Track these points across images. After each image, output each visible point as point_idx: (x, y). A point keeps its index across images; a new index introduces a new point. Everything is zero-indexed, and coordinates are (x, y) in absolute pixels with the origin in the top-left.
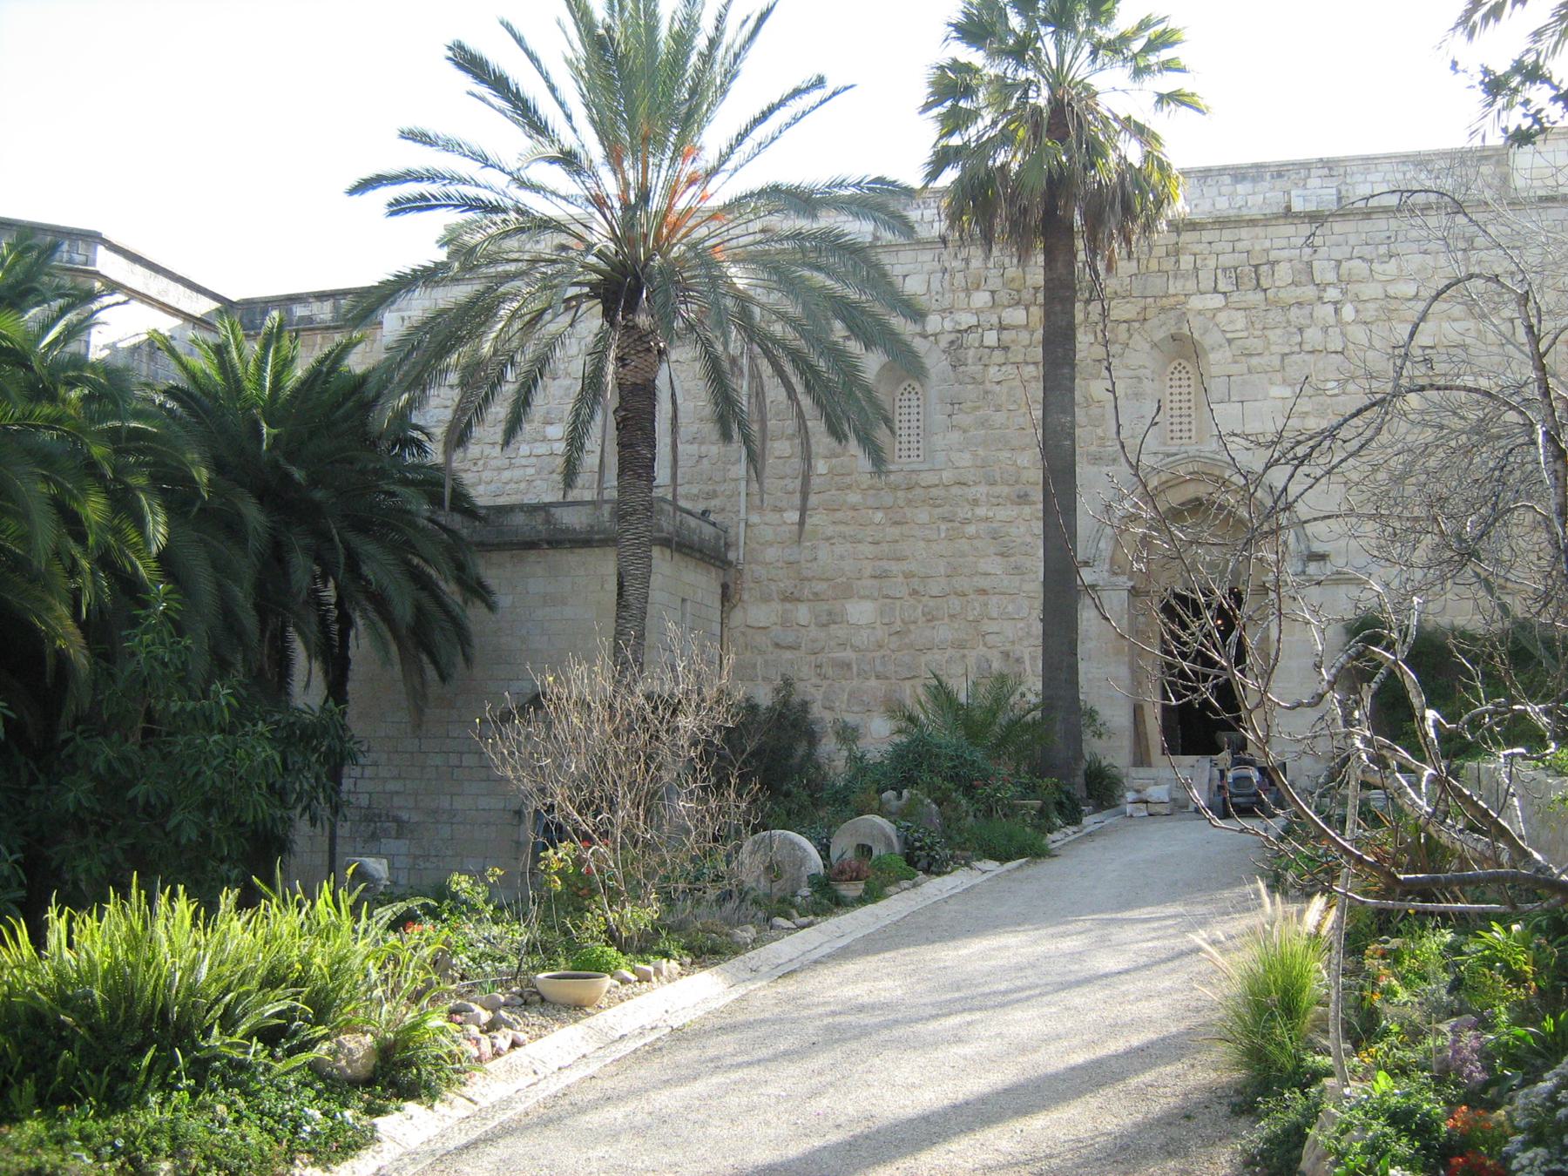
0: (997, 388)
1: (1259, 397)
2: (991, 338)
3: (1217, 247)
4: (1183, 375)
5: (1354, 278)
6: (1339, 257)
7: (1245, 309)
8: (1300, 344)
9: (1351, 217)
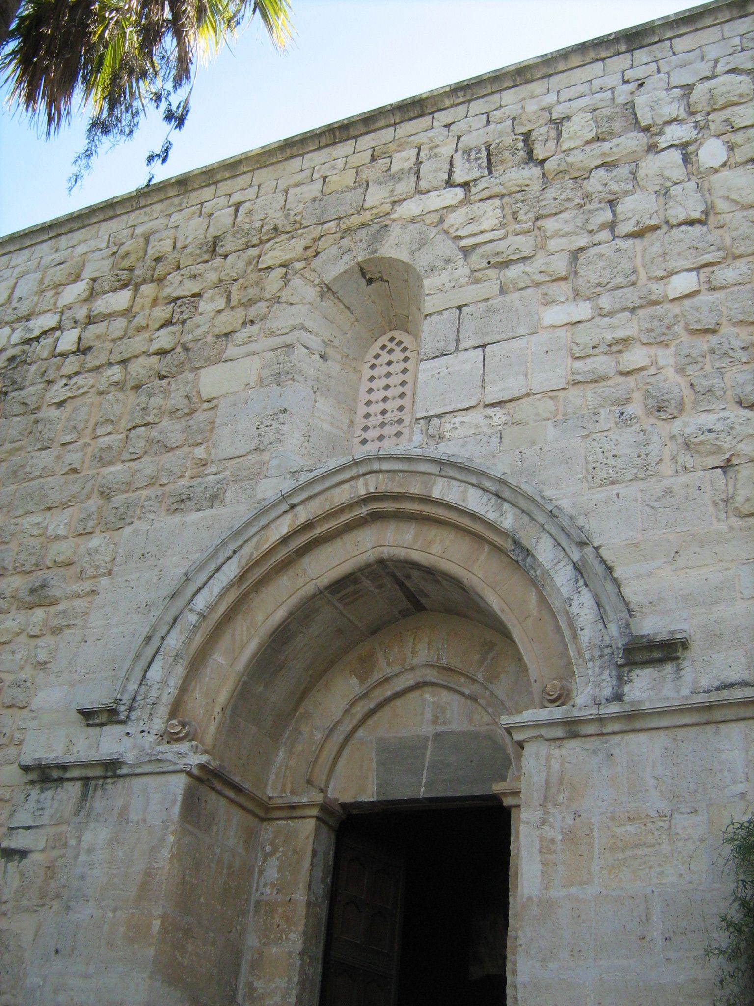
0: (54, 413)
1: (522, 331)
2: (68, 340)
3: (461, 126)
4: (398, 355)
5: (721, 101)
6: (689, 81)
7: (501, 196)
8: (612, 226)
9: (709, 21)
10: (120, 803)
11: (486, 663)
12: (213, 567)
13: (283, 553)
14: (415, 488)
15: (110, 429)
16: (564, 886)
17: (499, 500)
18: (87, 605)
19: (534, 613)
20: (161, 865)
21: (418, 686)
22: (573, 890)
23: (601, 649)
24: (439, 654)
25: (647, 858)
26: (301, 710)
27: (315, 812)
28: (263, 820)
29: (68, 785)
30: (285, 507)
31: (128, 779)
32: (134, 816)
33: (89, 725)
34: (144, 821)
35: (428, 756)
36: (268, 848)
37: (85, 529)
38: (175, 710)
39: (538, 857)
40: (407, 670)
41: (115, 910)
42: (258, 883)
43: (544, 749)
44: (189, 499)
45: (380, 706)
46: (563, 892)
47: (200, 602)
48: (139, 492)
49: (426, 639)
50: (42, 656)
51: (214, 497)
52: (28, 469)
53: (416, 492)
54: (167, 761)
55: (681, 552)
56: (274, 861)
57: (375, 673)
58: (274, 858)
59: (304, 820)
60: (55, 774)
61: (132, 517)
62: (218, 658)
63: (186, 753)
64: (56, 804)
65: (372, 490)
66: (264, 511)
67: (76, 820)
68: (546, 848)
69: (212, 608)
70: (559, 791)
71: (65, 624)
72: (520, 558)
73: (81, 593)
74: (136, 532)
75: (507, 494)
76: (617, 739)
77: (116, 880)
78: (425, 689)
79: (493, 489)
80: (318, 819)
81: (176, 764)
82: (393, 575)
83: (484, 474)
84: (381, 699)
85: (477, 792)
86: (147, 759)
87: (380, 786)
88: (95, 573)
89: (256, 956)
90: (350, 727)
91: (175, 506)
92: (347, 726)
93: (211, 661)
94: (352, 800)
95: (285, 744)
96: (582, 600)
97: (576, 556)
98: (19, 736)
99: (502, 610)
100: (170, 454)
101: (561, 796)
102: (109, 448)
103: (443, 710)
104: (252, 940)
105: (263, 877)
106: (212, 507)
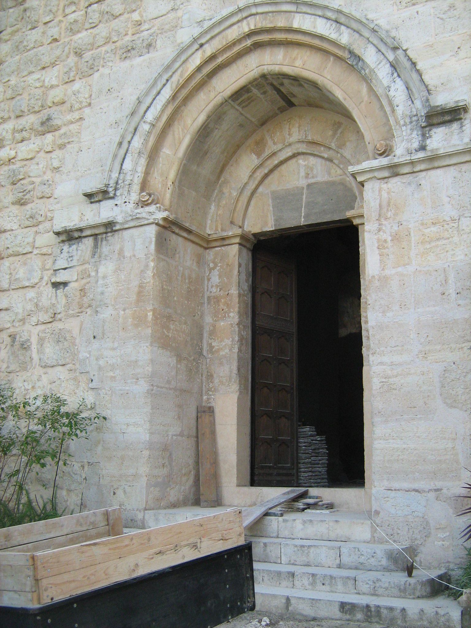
10: (117, 247)
11: (337, 137)
12: (154, 92)
13: (199, 77)
14: (281, 23)
15: (73, 8)
16: (394, 268)
17: (338, 25)
18: (78, 127)
19: (366, 98)
20: (148, 280)
21: (294, 156)
22: (400, 269)
23: (411, 118)
24: (306, 134)
25: (444, 246)
26: (222, 179)
27: (237, 240)
28: (206, 248)
29: (85, 241)
30: (196, 46)
31: (121, 232)
32: (127, 254)
33: (92, 203)
34: (134, 256)
35: (304, 199)
36: (212, 265)
37: (69, 78)
38: (144, 186)
39: (377, 252)
40: (286, 146)
41: (124, 310)
42: (207, 286)
43: (376, 184)
44: (133, 49)
45: (271, 171)
46: (393, 271)
47: (150, 116)
48: (100, 49)
49: (297, 125)
50: (56, 164)
51: (149, 45)
52: (25, 43)
53: (282, 25)
54: (143, 218)
55: (461, 48)
56: (216, 272)
57: (266, 150)
58: (216, 270)
59: (231, 246)
60: (76, 235)
61: (97, 66)
62: (166, 151)
63: (154, 212)
64: (79, 252)
65: (253, 28)
66: (183, 51)
67: (93, 260)
68: (382, 246)
69: (158, 119)
70: (387, 210)
71: (67, 141)
72: (354, 63)
73: (73, 121)
74: (102, 76)
75: (343, 19)
76: (424, 174)
77: (122, 292)
78: (299, 157)
79: (333, 17)
80: (240, 244)
81: (148, 219)
82: (272, 84)
83: (326, 8)
84: (271, 166)
85: (337, 218)
86: (130, 218)
87: (276, 220)
88: (80, 106)
89: (212, 328)
90: (254, 186)
91: (125, 55)
92: (252, 186)
93: (162, 153)
94: (260, 231)
95: (214, 201)
96: (396, 86)
97: (391, 57)
98: (50, 215)
99: (345, 99)
100: (116, 20)
101: (390, 213)
102: (76, 21)
103: (312, 169)
104: (208, 319)
105: (210, 283)
106: (149, 53)
